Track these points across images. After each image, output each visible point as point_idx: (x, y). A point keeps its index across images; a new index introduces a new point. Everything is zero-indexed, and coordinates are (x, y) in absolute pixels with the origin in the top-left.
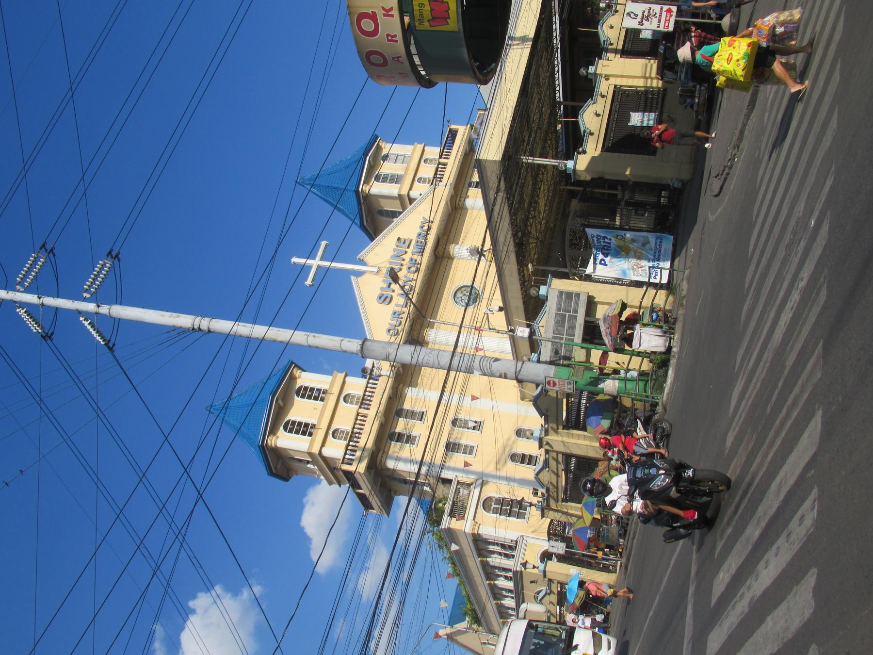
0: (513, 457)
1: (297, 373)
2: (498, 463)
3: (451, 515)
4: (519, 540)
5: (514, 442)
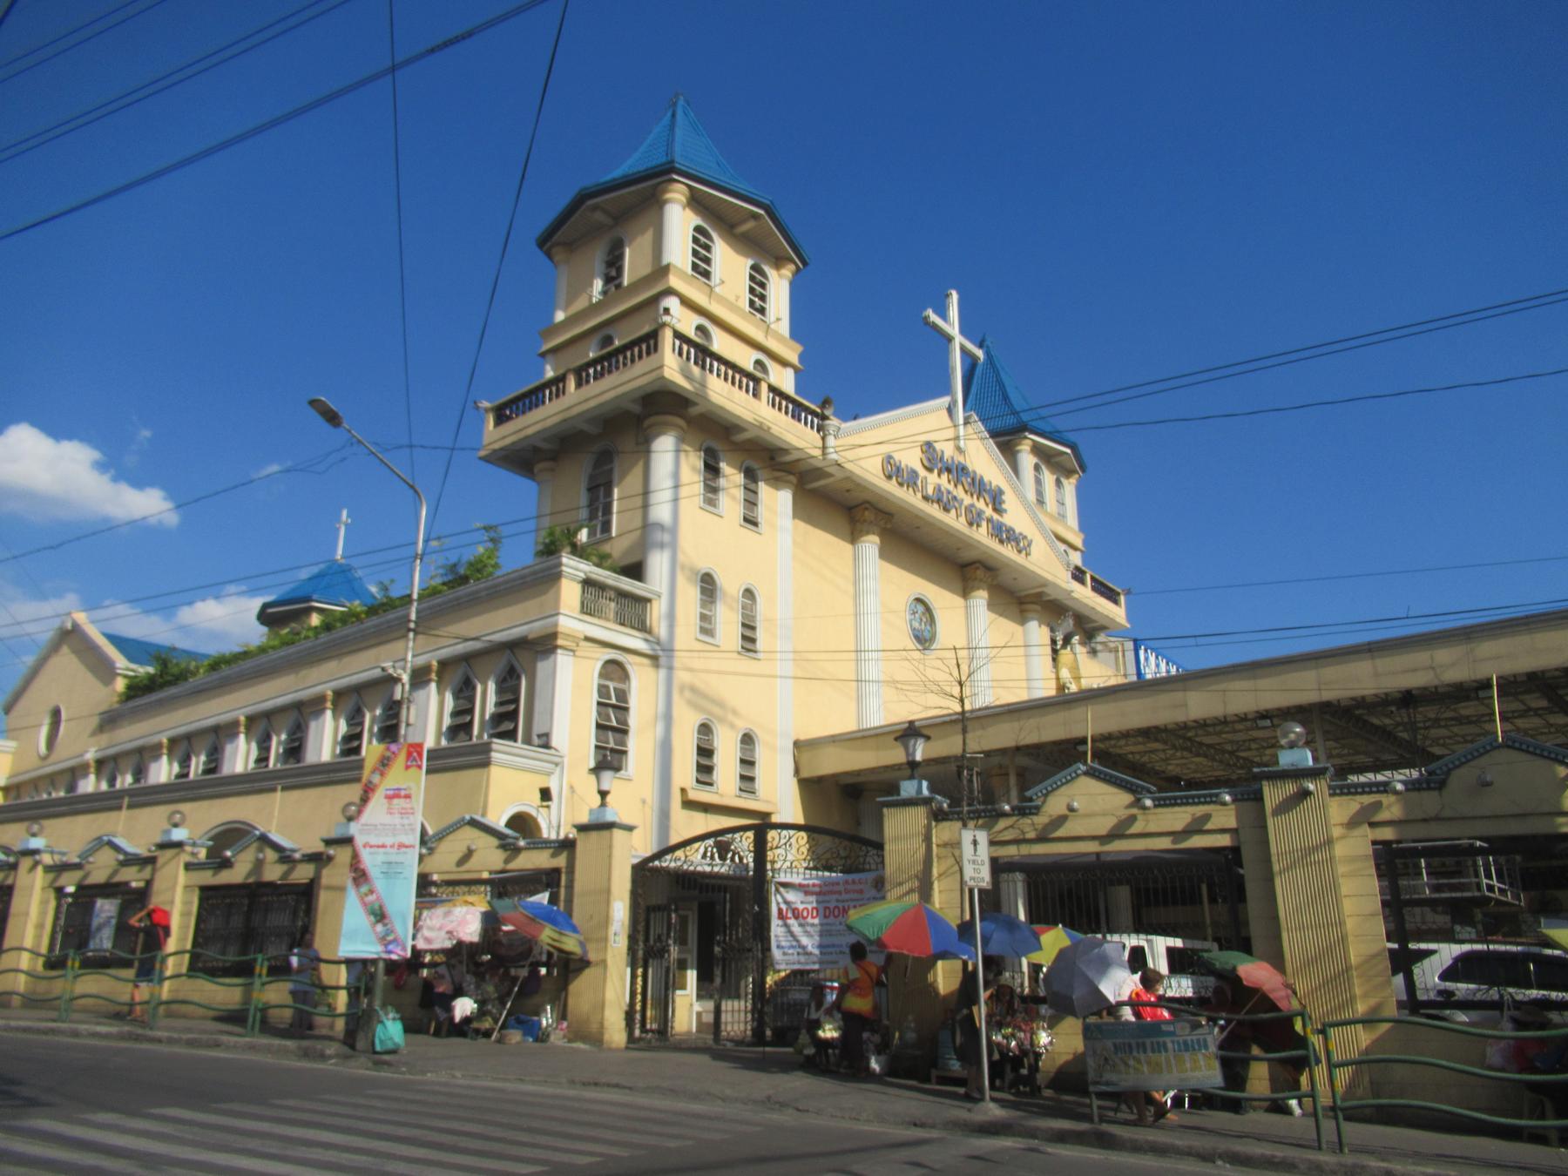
0: (705, 729)
1: (788, 271)
2: (693, 689)
3: (588, 583)
4: (552, 752)
5: (732, 726)
